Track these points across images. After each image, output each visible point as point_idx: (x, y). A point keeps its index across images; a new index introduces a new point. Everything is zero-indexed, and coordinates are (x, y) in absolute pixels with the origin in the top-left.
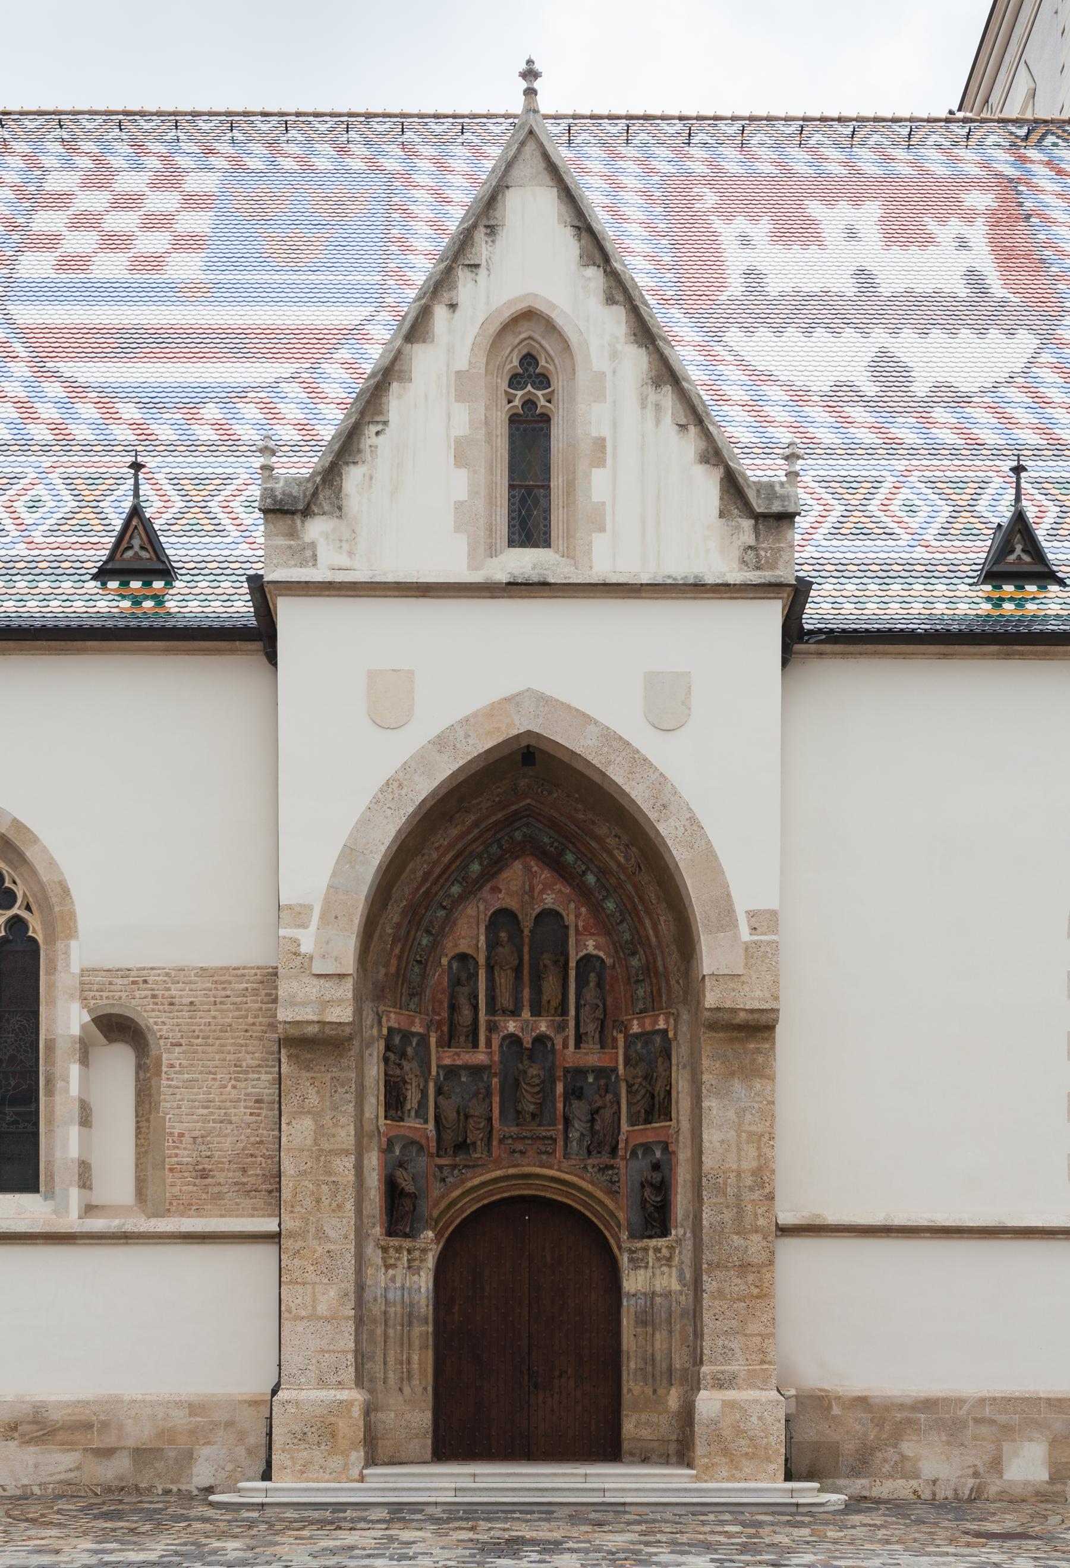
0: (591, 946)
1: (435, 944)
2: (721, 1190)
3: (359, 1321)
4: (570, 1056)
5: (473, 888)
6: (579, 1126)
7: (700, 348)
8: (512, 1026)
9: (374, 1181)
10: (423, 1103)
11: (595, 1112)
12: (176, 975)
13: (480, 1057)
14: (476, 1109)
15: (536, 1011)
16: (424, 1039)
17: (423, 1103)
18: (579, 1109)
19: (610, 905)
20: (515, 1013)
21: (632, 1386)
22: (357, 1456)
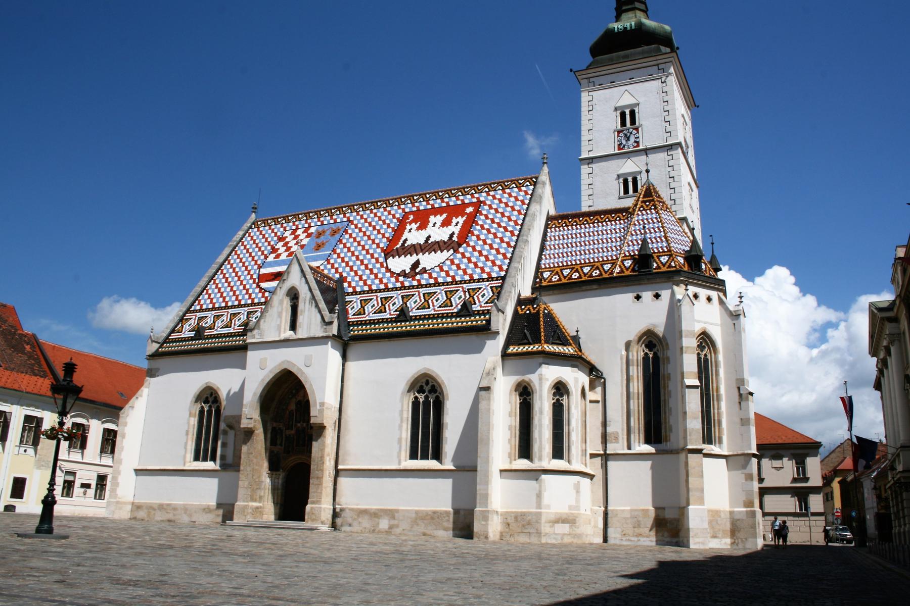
2: (314, 461)
7: (382, 264)
8: (299, 425)
10: (282, 442)
15: (303, 422)
17: (282, 442)
20: (300, 422)
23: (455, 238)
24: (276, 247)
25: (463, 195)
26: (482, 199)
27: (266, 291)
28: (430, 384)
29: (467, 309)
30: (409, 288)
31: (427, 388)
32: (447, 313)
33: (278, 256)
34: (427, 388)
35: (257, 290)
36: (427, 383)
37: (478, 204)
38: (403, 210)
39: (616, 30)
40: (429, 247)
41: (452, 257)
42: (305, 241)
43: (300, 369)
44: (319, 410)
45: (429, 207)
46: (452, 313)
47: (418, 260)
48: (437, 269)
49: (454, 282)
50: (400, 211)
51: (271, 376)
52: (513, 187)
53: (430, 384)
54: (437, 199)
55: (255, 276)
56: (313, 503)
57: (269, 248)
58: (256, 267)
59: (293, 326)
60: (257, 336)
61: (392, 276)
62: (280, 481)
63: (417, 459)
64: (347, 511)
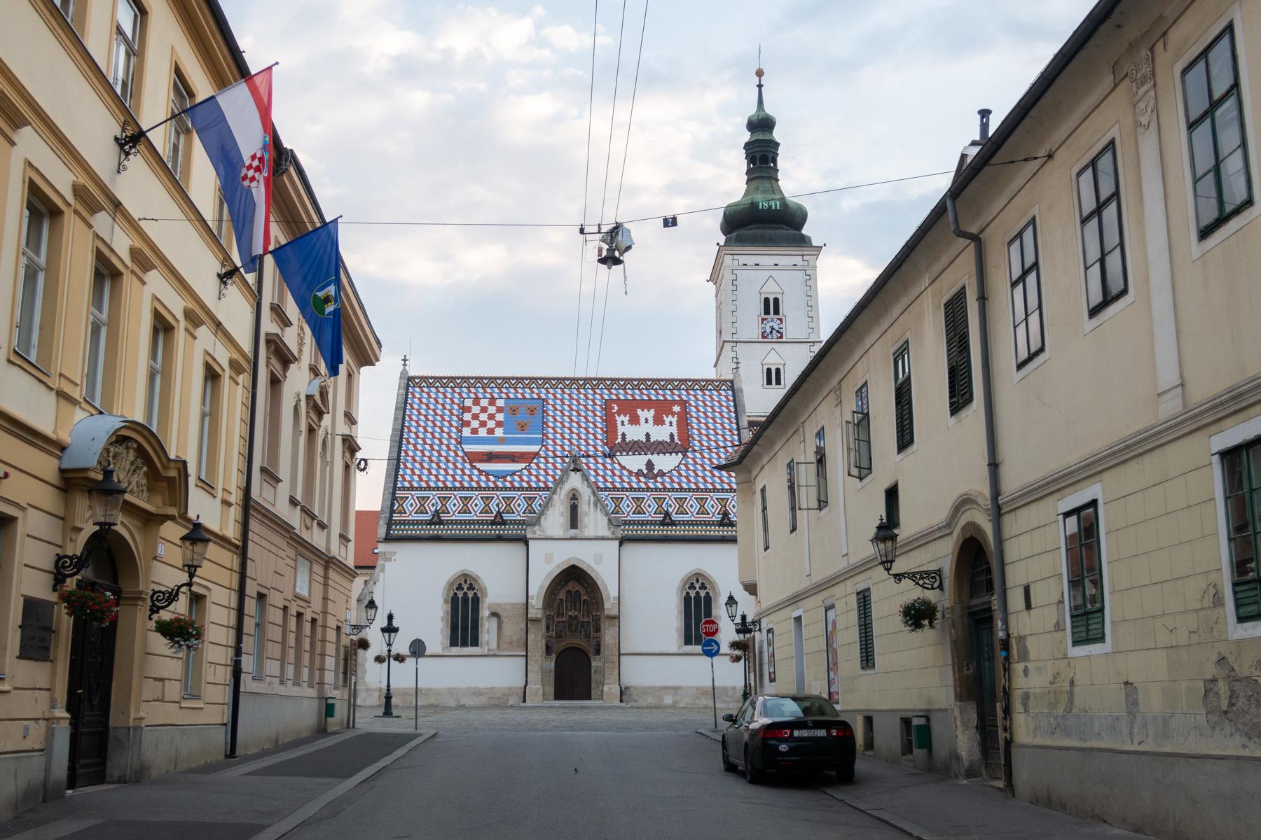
0: (585, 597)
1: (556, 598)
3: (542, 671)
4: (582, 619)
5: (563, 586)
6: (583, 633)
9: (544, 645)
11: (586, 630)
12: (506, 604)
13: (564, 620)
14: (564, 630)
15: (575, 610)
16: (553, 616)
18: (583, 629)
19: (589, 590)
20: (571, 610)
21: (593, 685)
22: (542, 698)
23: (676, 440)
24: (465, 419)
25: (660, 389)
26: (684, 398)
27: (487, 474)
28: (700, 582)
29: (729, 519)
30: (656, 489)
31: (698, 586)
32: (705, 521)
33: (474, 431)
34: (698, 586)
35: (475, 472)
36: (697, 581)
37: (683, 403)
38: (601, 395)
39: (761, 207)
40: (647, 446)
41: (683, 462)
42: (500, 417)
43: (588, 565)
44: (613, 604)
45: (630, 397)
46: (713, 521)
47: (649, 461)
48: (675, 473)
49: (698, 489)
50: (598, 397)
51: (559, 571)
52: (711, 390)
53: (700, 582)
54: (633, 389)
55: (460, 453)
56: (609, 684)
57: (455, 418)
58: (453, 441)
59: (574, 523)
60: (538, 533)
61: (631, 475)
62: (553, 664)
63: (691, 644)
64: (632, 689)
